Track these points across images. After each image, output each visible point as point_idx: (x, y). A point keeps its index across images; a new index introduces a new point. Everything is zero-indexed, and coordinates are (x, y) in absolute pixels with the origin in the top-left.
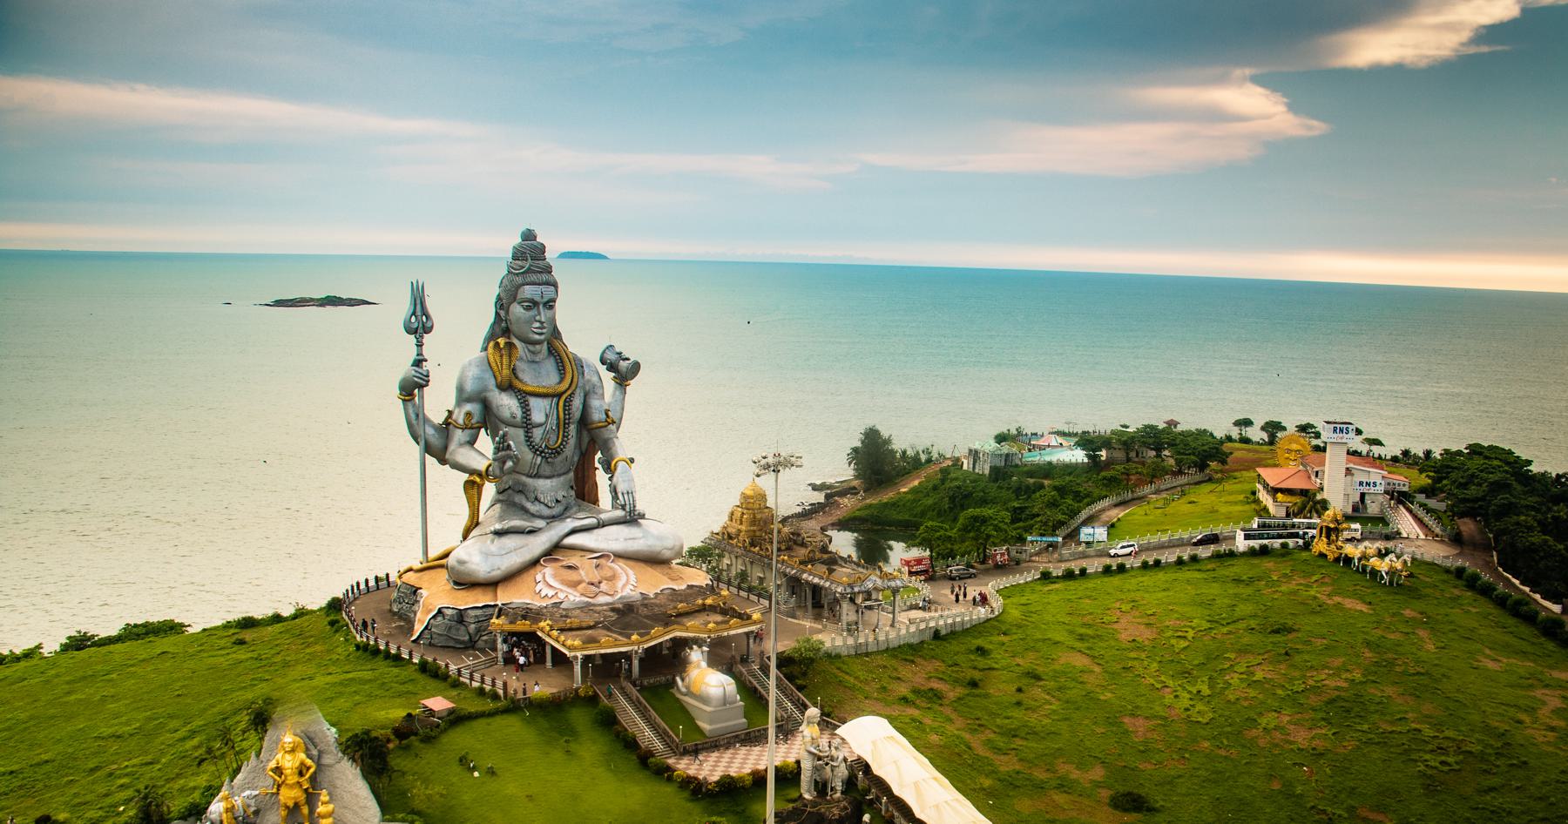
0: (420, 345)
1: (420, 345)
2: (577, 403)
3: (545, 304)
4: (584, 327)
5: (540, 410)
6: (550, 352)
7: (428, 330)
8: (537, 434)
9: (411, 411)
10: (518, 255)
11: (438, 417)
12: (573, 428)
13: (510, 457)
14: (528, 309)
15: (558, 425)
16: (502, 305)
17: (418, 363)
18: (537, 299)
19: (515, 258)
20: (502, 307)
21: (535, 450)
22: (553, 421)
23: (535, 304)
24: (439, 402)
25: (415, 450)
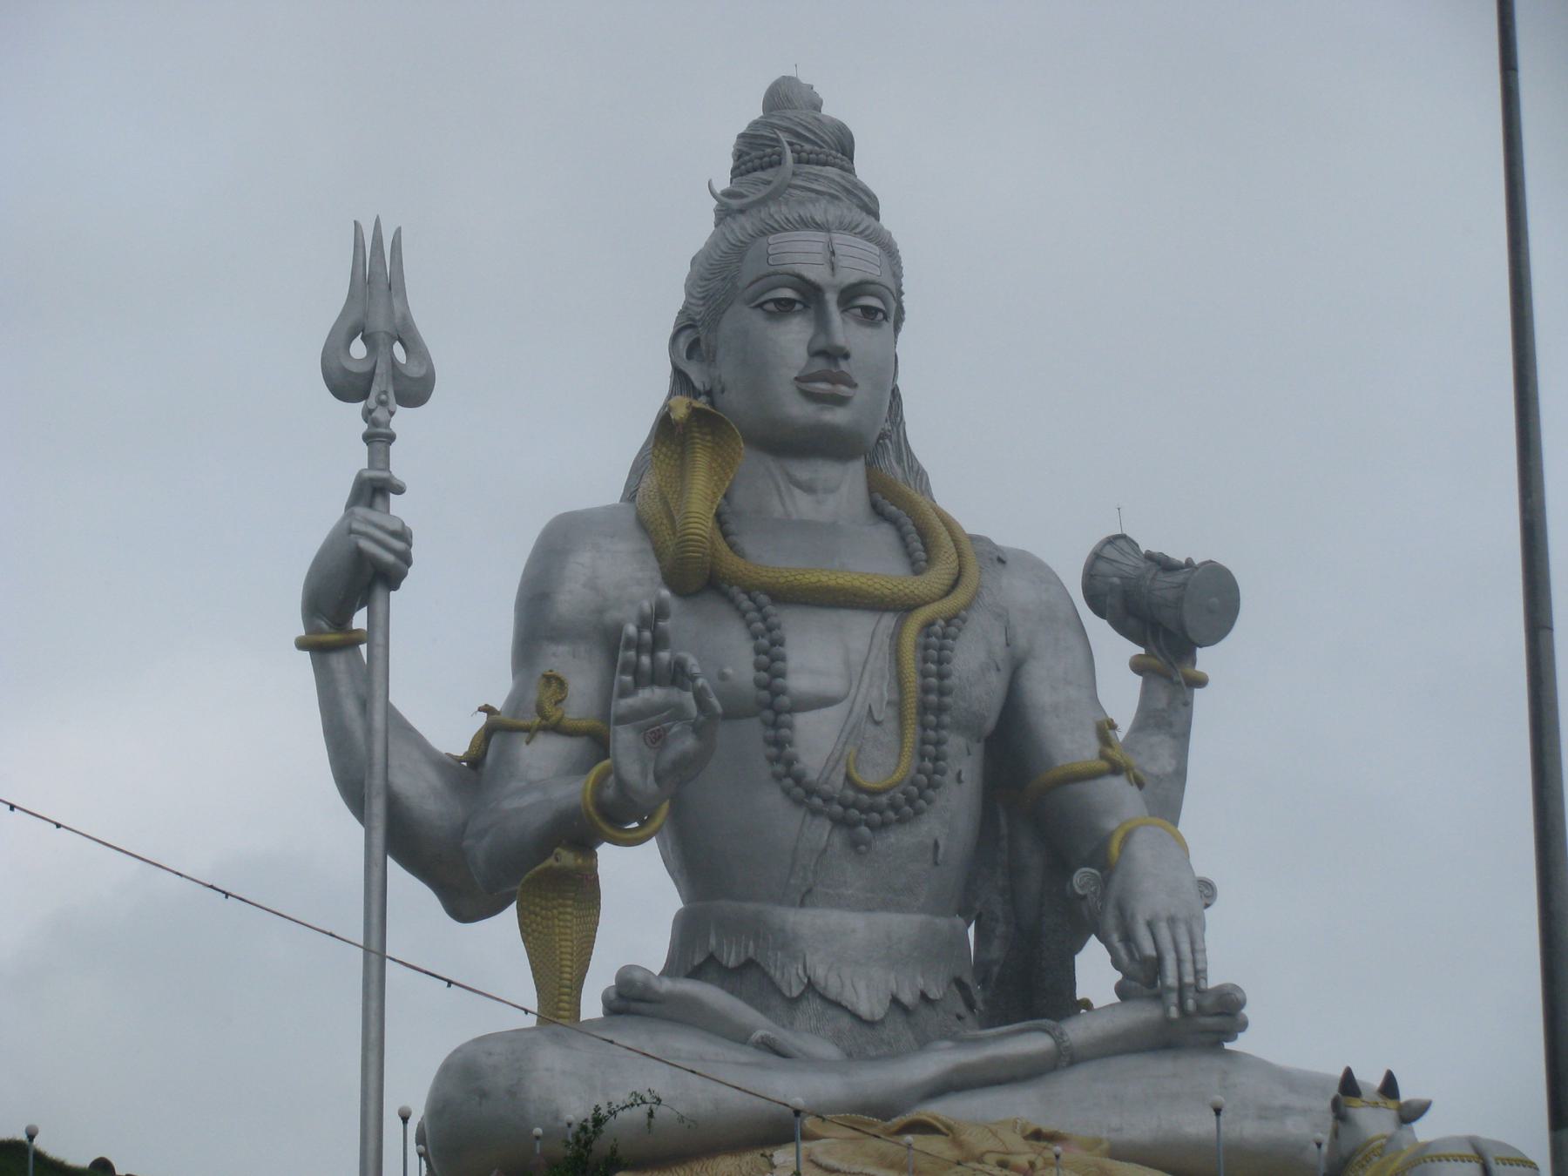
0: (378, 438)
1: (378, 438)
2: (971, 657)
3: (849, 296)
4: (1016, 440)
5: (820, 655)
6: (878, 512)
7: (415, 391)
8: (816, 739)
9: (345, 687)
10: (755, 153)
11: (453, 736)
12: (964, 761)
13: (677, 712)
14: (784, 308)
16: (695, 337)
17: (374, 490)
18: (816, 273)
19: (736, 172)
20: (693, 349)
21: (802, 792)
22: (876, 691)
23: (809, 296)
24: (449, 668)
25: (343, 838)
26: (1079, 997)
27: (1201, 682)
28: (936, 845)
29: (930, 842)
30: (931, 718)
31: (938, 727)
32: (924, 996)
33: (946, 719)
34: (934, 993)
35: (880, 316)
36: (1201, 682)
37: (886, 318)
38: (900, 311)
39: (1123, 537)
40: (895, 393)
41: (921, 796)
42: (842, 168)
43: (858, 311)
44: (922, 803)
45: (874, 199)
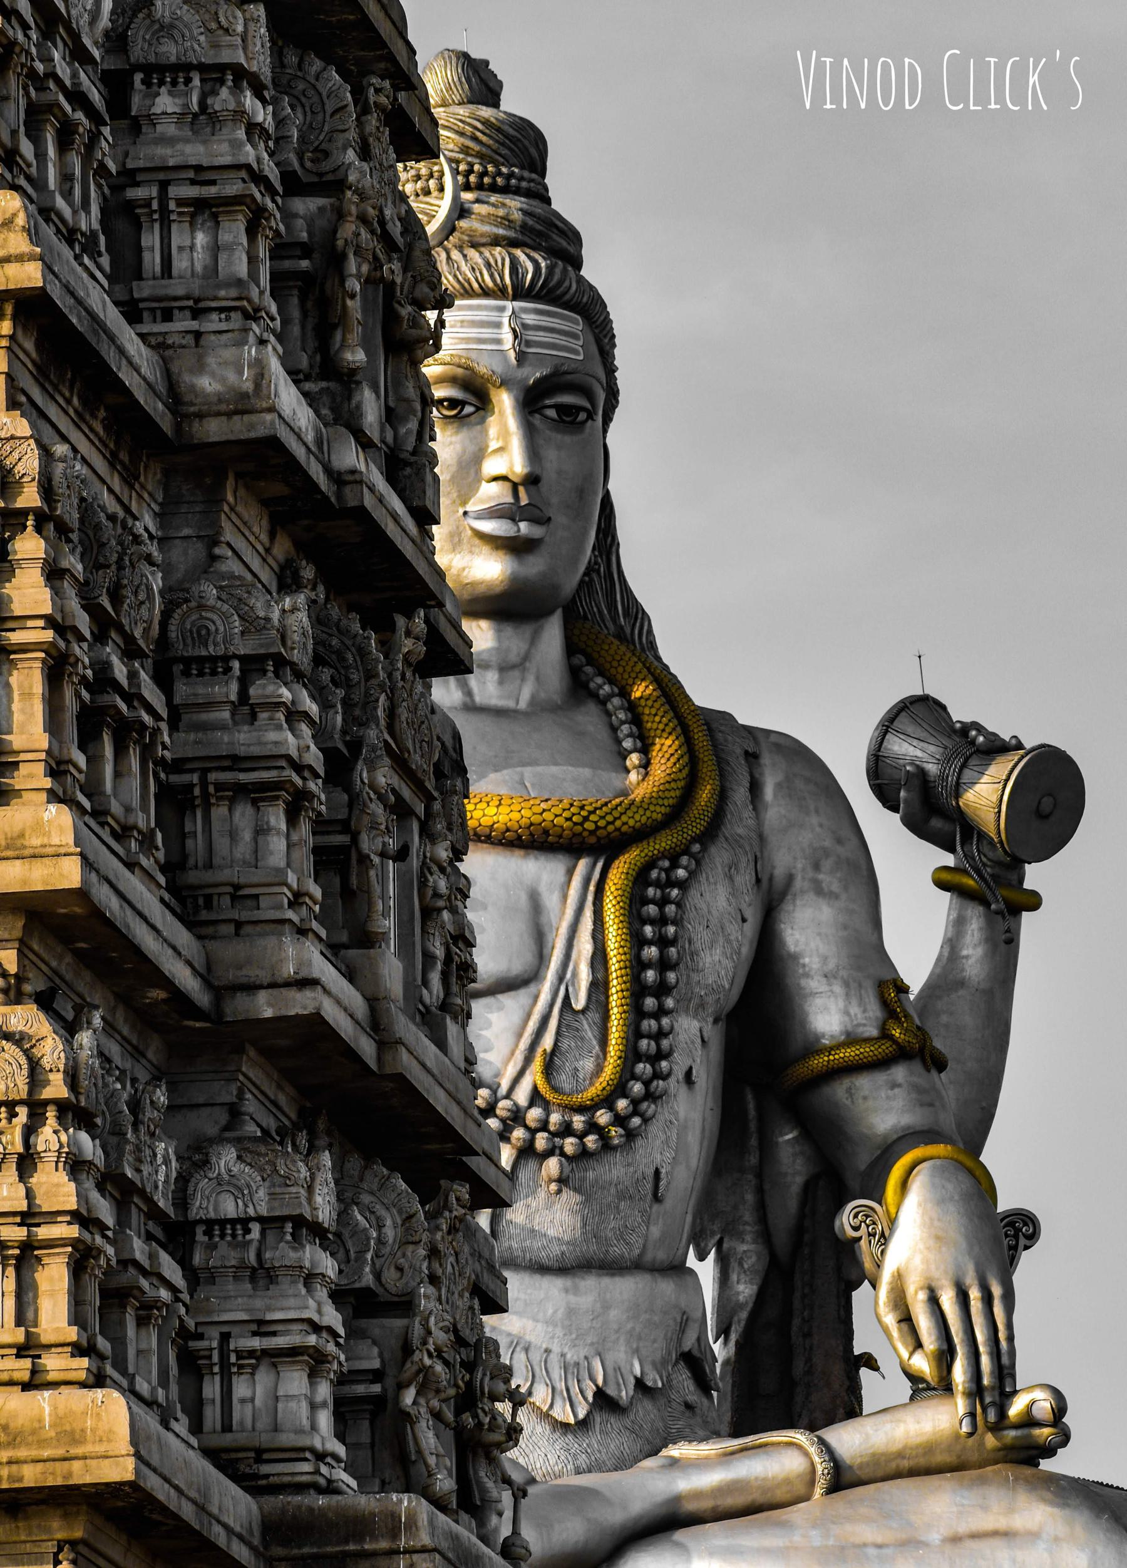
15: (599, 986)
26: (857, 1351)
27: (1034, 902)
28: (657, 1172)
29: (650, 1172)
30: (650, 1002)
31: (661, 1012)
32: (640, 1383)
33: (670, 1003)
34: (654, 1380)
35: (582, 416)
36: (1034, 902)
37: (591, 416)
38: (613, 394)
39: (924, 699)
40: (607, 505)
41: (635, 1113)
42: (528, 194)
43: (552, 413)
44: (636, 1121)
45: (575, 238)
